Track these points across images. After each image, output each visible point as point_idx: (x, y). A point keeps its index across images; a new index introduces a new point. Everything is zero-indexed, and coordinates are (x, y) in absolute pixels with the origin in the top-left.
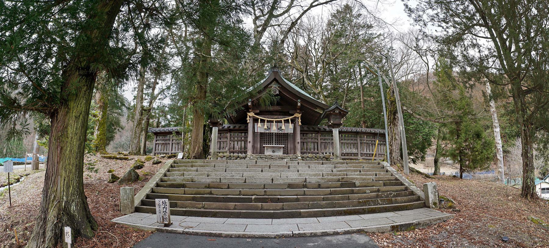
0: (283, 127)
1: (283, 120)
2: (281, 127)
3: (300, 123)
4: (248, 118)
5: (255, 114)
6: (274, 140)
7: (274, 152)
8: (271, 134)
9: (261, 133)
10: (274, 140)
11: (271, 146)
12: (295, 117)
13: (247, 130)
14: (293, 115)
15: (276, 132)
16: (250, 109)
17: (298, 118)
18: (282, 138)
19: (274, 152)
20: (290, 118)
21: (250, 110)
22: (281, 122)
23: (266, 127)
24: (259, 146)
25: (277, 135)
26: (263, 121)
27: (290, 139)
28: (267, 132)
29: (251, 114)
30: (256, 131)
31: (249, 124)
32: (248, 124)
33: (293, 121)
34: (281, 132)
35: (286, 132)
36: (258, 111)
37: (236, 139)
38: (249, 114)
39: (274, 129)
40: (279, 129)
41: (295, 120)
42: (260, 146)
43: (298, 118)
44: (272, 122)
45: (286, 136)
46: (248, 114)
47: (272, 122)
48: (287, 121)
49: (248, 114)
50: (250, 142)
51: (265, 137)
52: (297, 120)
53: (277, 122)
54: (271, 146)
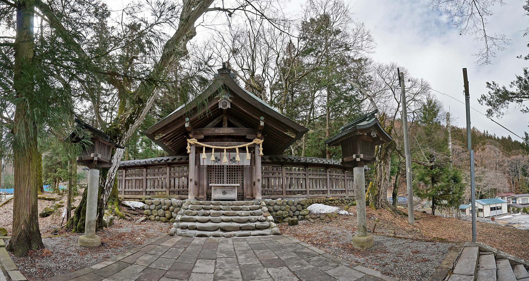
0: (238, 158)
1: (237, 147)
2: (234, 158)
3: (261, 153)
4: (188, 147)
5: (199, 141)
6: (225, 175)
7: (224, 193)
8: (221, 167)
9: (208, 166)
10: (225, 175)
11: (222, 185)
12: (255, 144)
13: (188, 163)
14: (251, 141)
15: (228, 164)
16: (190, 132)
17: (259, 145)
18: (235, 171)
19: (224, 193)
20: (247, 145)
21: (191, 136)
22: (234, 150)
23: (213, 158)
24: (205, 183)
25: (230, 168)
26: (208, 150)
27: (246, 174)
28: (217, 164)
29: (192, 141)
30: (201, 164)
31: (190, 156)
32: (188, 154)
33: (252, 149)
34: (234, 164)
35: (241, 164)
36: (202, 137)
37: (177, 174)
38: (189, 141)
39: (225, 161)
40: (231, 160)
41: (254, 148)
42: (208, 184)
43: (259, 145)
44: (222, 150)
45: (241, 168)
46: (188, 140)
47: (222, 150)
48: (243, 150)
49: (188, 140)
50: (191, 180)
51: (214, 171)
52: (257, 148)
53: (228, 151)
54: (222, 185)
